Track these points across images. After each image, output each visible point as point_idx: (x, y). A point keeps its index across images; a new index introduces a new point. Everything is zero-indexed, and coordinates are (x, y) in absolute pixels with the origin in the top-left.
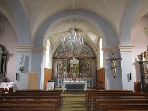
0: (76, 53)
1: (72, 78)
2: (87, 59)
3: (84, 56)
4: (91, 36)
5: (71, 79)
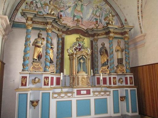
1: (75, 90)
5: (72, 93)
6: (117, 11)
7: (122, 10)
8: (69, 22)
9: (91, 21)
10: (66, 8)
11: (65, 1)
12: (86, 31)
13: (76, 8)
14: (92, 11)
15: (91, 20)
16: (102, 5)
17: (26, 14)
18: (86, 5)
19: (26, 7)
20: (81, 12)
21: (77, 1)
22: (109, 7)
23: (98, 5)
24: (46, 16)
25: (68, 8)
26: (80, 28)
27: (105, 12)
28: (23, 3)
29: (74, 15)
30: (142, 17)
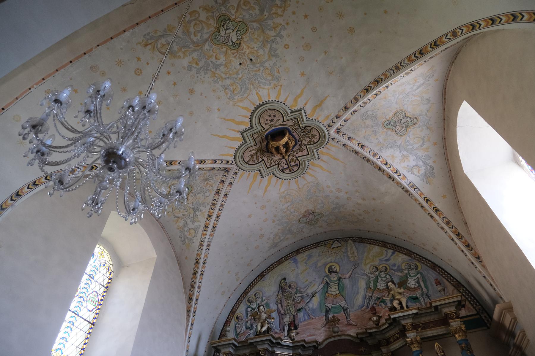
0: (345, 310)
2: (426, 326)
3: (393, 309)
4: (386, 154)
6: (429, 258)
7: (433, 252)
8: (319, 330)
9: (367, 310)
10: (307, 299)
11: (303, 287)
12: (358, 341)
13: (327, 291)
14: (367, 285)
15: (368, 307)
16: (387, 260)
17: (219, 348)
18: (348, 276)
19: (237, 325)
20: (341, 297)
21: (327, 276)
22: (405, 256)
23: (376, 263)
24: (255, 340)
25: (311, 299)
26: (343, 337)
27: (400, 274)
28: (232, 319)
29: (326, 309)
30: (478, 258)
